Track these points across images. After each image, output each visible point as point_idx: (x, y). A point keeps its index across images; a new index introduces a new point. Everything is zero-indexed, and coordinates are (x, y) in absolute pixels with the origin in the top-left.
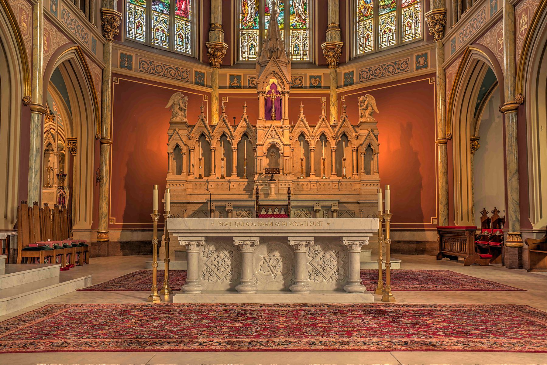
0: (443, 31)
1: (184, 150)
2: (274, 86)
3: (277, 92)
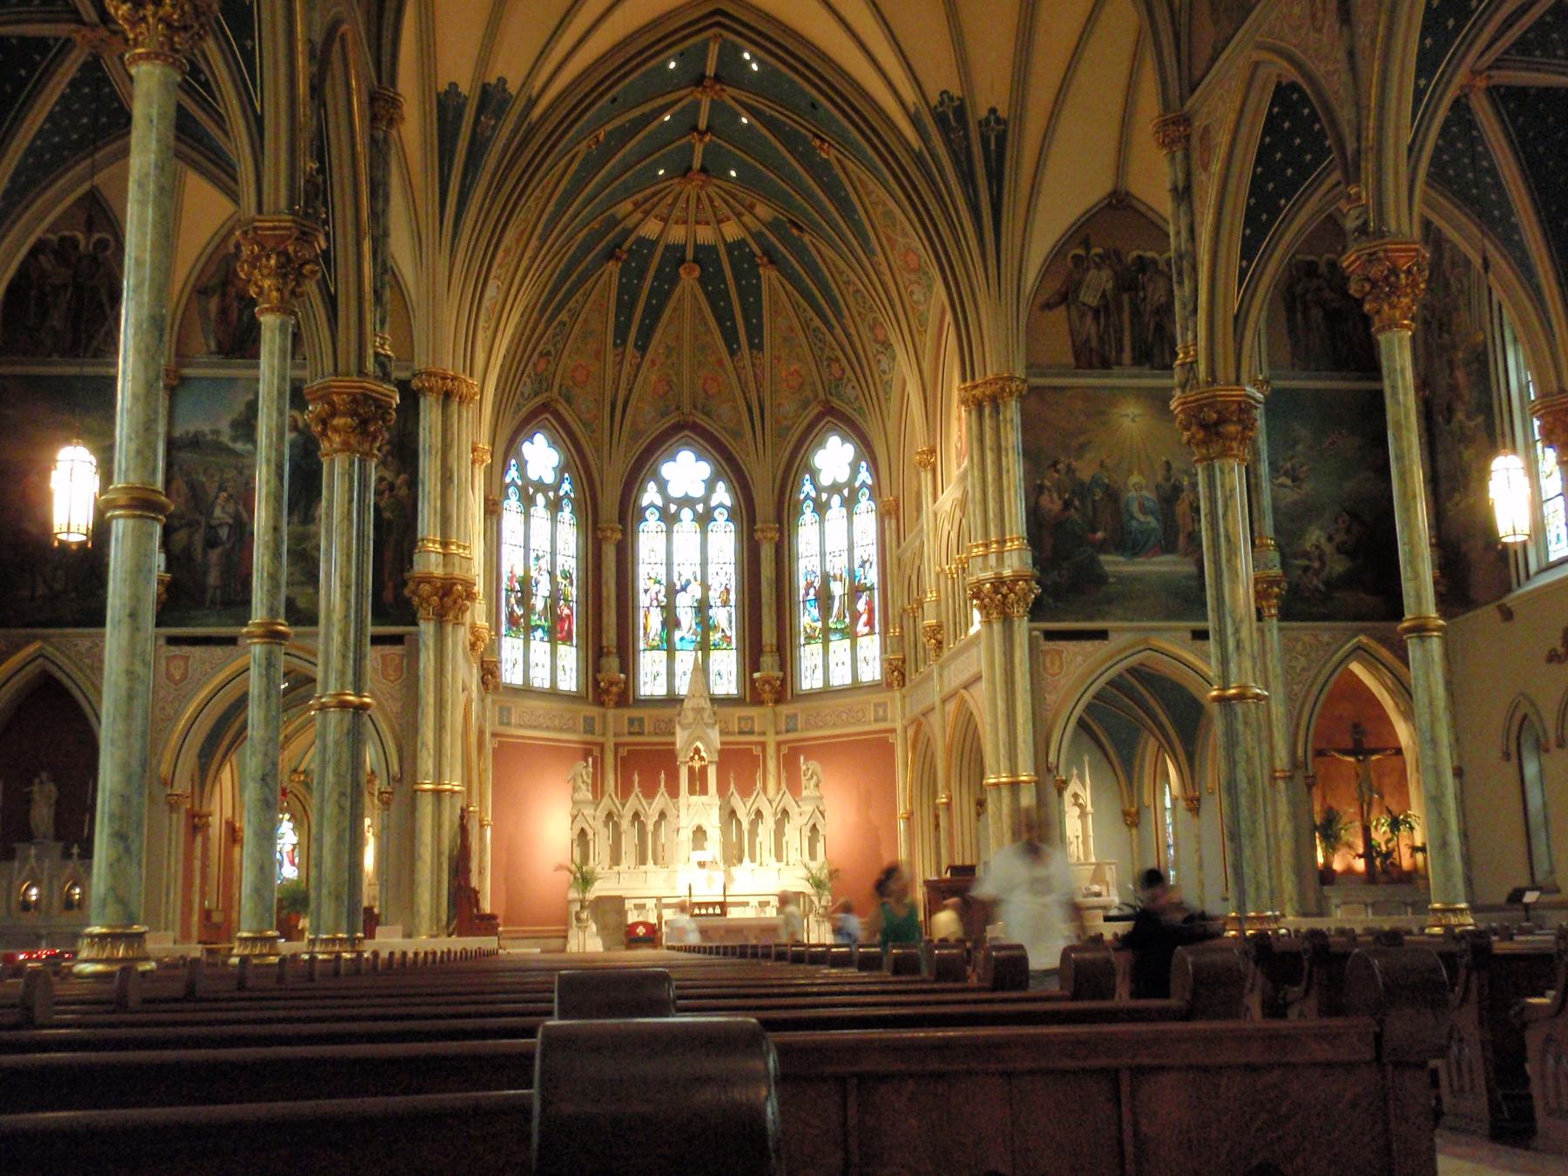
0: (902, 683)
1: (590, 836)
3: (702, 759)
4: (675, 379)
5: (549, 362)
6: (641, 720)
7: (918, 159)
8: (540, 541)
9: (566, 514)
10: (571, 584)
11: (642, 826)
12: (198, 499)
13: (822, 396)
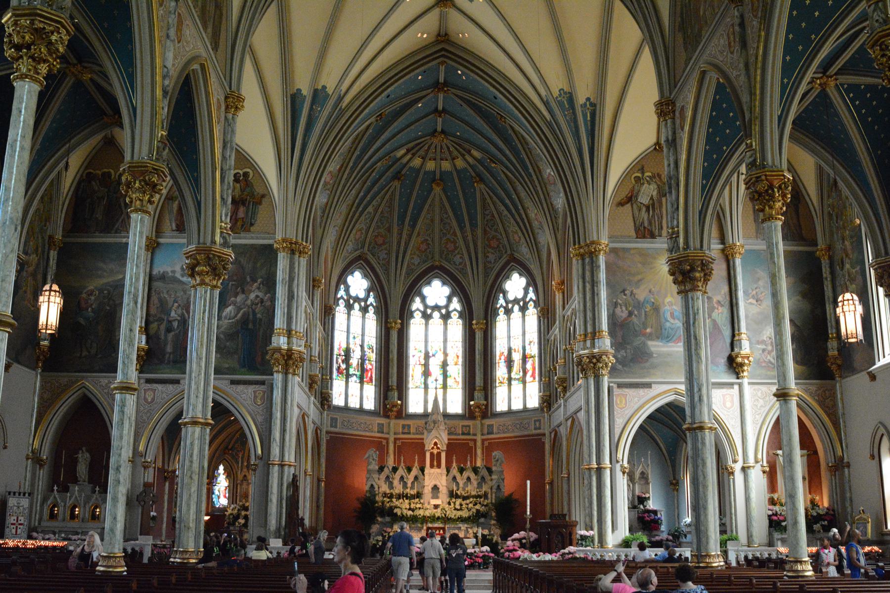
0: (549, 406)
3: (438, 448)
4: (431, 243)
5: (362, 233)
6: (409, 426)
7: (549, 125)
8: (356, 328)
9: (371, 315)
10: (373, 352)
12: (164, 307)
13: (509, 252)
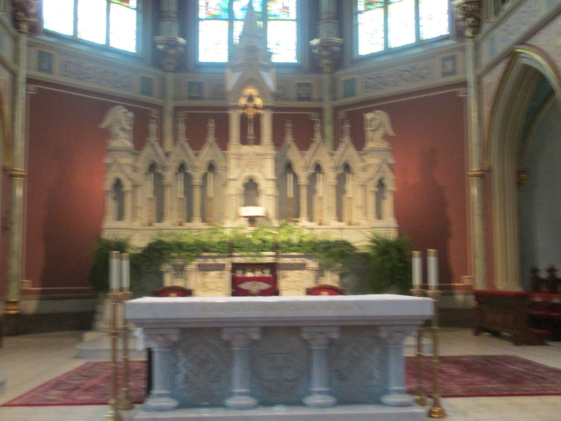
0: (476, 27)
1: (127, 186)
2: (250, 98)
11: (188, 178)
